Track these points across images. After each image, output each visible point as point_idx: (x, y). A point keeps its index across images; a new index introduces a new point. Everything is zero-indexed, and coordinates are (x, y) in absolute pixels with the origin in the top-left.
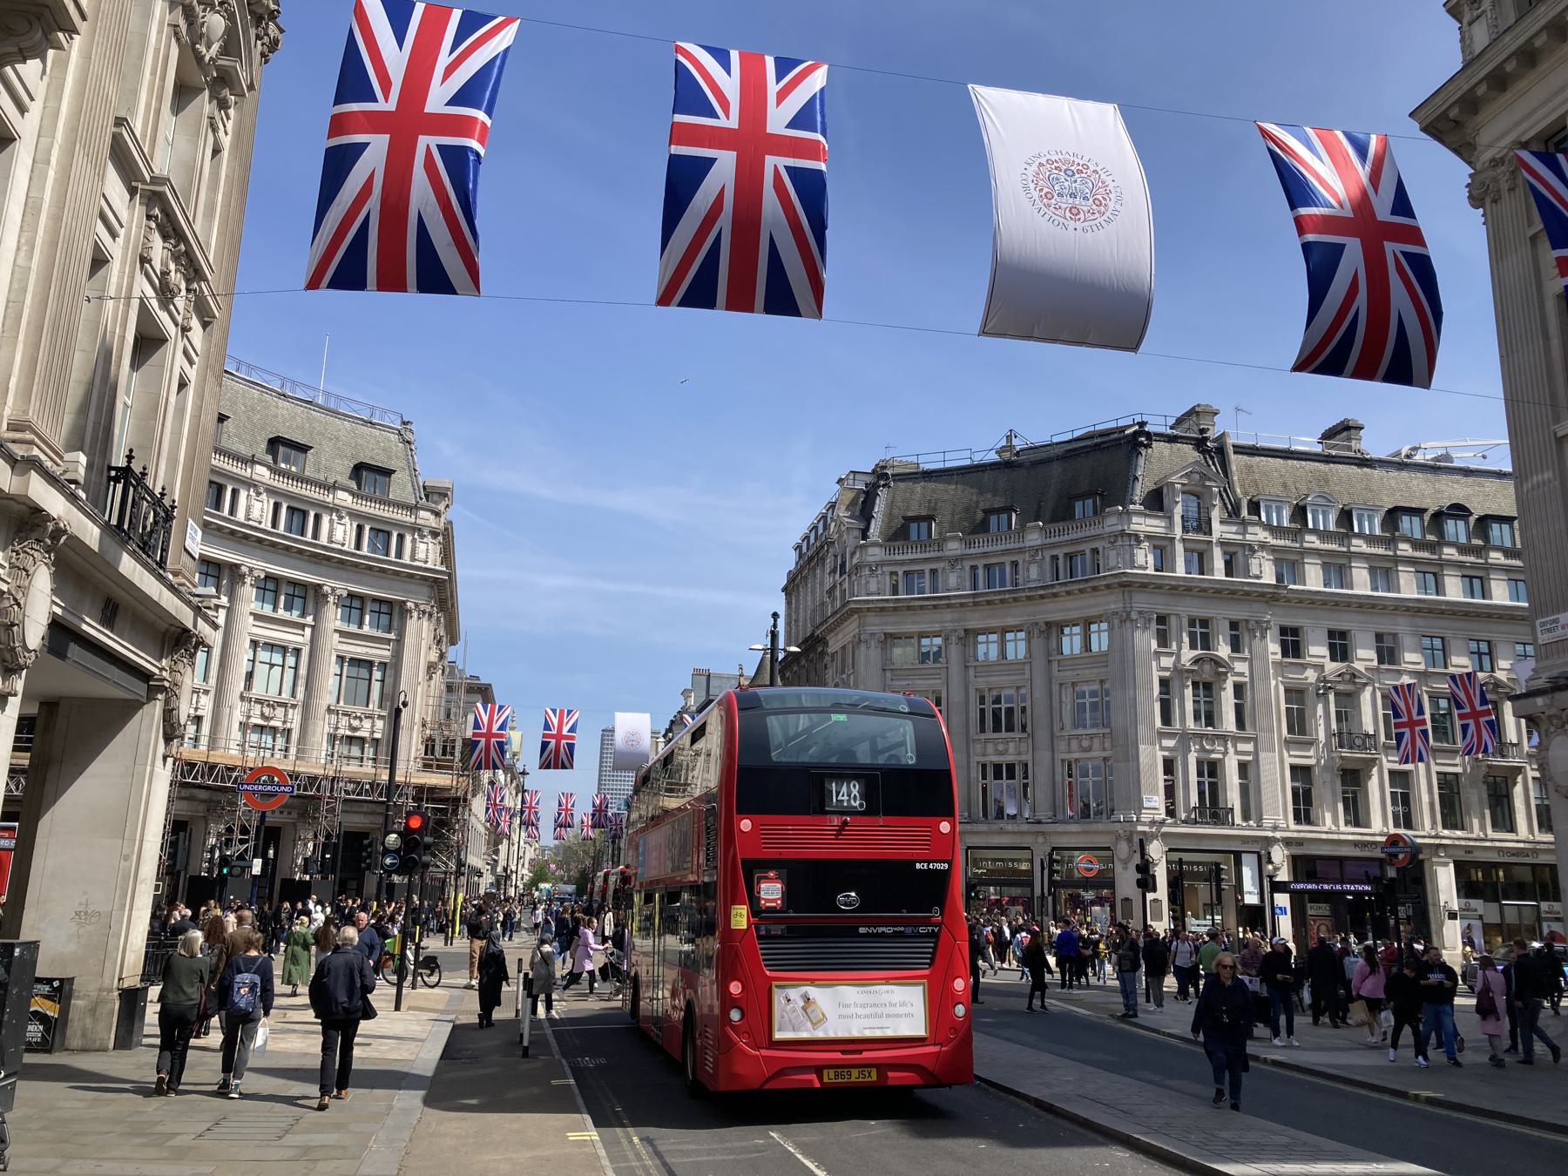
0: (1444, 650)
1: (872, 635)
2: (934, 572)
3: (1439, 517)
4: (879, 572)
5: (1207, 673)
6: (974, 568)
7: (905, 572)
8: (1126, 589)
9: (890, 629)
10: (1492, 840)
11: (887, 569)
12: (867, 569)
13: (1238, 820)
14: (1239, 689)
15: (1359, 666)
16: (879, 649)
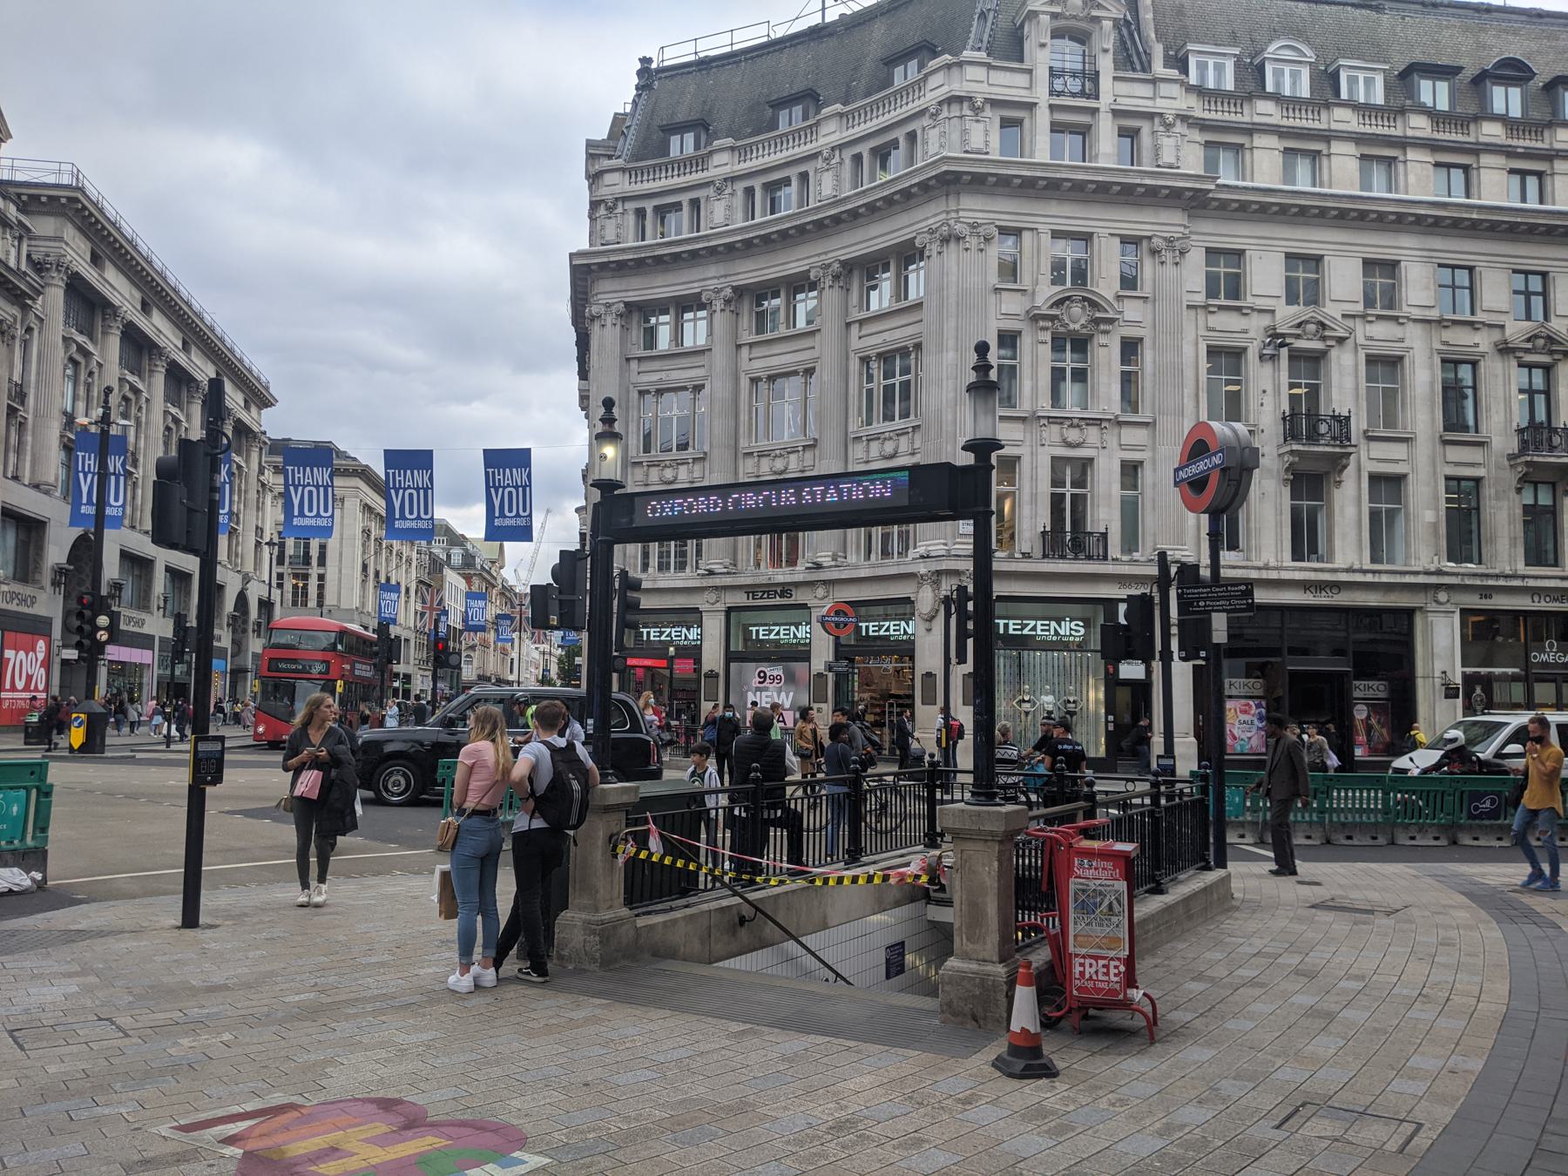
0: (1471, 288)
1: (608, 306)
2: (695, 203)
3: (1481, 80)
4: (620, 210)
5: (1077, 319)
6: (750, 192)
7: (655, 207)
8: (952, 187)
9: (633, 297)
10: (1524, 577)
11: (631, 206)
12: (603, 206)
13: (1114, 550)
14: (1130, 348)
15: (1332, 311)
16: (618, 327)
